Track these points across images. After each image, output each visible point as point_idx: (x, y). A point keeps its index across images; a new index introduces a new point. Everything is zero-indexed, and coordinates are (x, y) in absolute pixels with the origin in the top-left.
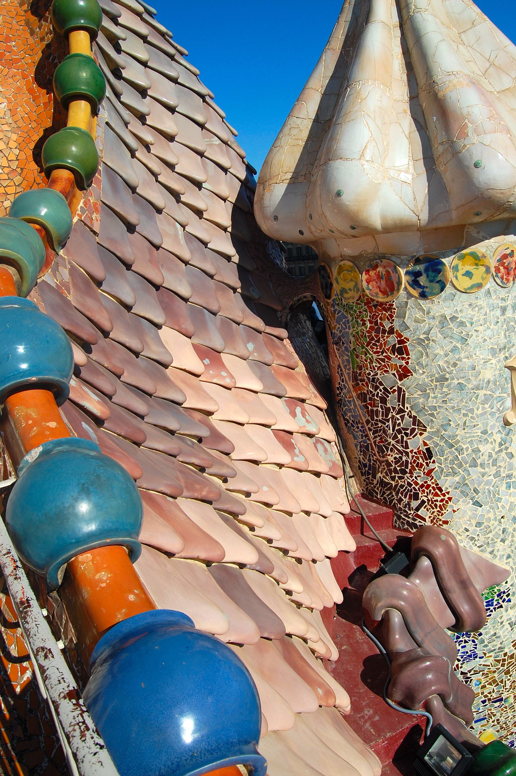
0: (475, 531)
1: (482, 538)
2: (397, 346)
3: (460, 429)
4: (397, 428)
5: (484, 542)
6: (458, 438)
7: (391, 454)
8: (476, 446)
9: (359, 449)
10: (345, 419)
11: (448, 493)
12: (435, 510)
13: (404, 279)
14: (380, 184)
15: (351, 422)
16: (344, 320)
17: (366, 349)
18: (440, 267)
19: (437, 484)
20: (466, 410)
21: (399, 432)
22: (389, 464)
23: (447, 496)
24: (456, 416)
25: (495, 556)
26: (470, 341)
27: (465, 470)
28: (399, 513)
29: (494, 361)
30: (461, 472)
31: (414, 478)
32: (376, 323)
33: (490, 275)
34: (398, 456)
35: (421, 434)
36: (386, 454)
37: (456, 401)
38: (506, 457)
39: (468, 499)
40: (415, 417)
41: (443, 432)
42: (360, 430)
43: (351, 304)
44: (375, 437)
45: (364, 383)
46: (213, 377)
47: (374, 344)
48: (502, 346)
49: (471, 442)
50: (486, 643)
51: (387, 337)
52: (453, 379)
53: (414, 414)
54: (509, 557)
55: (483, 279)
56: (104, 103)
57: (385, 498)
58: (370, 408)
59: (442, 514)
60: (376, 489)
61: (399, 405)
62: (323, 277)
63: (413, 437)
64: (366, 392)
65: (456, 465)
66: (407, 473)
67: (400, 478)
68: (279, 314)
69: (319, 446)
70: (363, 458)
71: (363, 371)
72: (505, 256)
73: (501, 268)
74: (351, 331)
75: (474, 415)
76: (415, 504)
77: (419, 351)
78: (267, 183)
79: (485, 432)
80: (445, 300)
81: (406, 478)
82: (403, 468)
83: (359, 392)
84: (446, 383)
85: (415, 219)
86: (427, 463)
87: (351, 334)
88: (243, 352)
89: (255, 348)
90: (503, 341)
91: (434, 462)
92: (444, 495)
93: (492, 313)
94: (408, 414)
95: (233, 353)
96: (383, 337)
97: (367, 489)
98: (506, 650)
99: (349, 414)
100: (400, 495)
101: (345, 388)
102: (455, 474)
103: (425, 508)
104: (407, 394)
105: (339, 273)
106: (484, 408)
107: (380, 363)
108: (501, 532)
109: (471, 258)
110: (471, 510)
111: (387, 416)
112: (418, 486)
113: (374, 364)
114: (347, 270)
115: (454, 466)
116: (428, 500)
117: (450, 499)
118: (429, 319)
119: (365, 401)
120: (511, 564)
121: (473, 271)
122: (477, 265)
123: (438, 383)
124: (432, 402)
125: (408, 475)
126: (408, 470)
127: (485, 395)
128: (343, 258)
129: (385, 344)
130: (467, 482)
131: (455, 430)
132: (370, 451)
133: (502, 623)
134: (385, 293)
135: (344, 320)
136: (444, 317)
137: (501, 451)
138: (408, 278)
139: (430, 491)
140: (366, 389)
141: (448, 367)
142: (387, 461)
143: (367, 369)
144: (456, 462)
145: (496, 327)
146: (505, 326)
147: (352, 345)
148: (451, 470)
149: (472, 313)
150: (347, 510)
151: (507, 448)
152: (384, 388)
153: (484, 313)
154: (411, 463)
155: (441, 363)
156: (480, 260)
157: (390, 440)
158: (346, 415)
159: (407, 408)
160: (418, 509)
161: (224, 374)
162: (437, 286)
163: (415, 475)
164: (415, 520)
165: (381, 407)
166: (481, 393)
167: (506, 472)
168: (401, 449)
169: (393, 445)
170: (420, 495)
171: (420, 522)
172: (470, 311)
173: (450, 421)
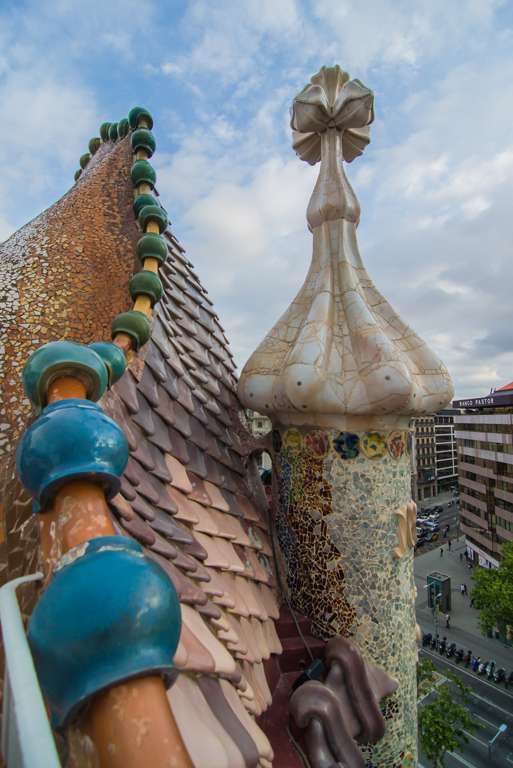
0: (373, 644)
1: (378, 651)
2: (324, 490)
3: (364, 557)
4: (319, 551)
5: (379, 654)
6: (363, 565)
7: (314, 572)
8: (375, 572)
9: (288, 565)
10: (280, 541)
11: (354, 609)
12: (344, 623)
13: (332, 445)
14: (324, 382)
15: (284, 543)
16: (287, 468)
17: (302, 490)
18: (356, 440)
19: (346, 601)
20: (369, 544)
21: (320, 555)
22: (311, 580)
23: (353, 611)
24: (362, 547)
25: (387, 669)
26: (373, 493)
27: (367, 591)
28: (316, 623)
29: (388, 509)
30: (364, 592)
31: (329, 593)
32: (310, 472)
33: (387, 450)
34: (318, 574)
35: (336, 559)
36: (309, 572)
37: (363, 536)
38: (395, 583)
39: (368, 615)
40: (333, 545)
41: (352, 559)
42: (291, 551)
43: (294, 457)
44: (302, 557)
45: (298, 515)
46: (197, 497)
47: (307, 487)
48: (393, 499)
49: (371, 569)
50: (379, 753)
51: (317, 483)
52: (360, 519)
53: (332, 542)
54: (397, 670)
55: (383, 451)
56: (158, 303)
57: (305, 609)
58: (300, 534)
59: (349, 627)
60: (299, 600)
61: (322, 534)
62: (276, 437)
63: (331, 560)
64: (298, 521)
65: (360, 586)
66: (324, 589)
67: (319, 593)
68: (242, 459)
69: (262, 560)
70: (291, 574)
71: (298, 506)
72: (396, 439)
73: (394, 446)
74: (291, 476)
75: (375, 548)
76: (328, 616)
77: (339, 496)
78: (248, 373)
79: (381, 562)
80: (358, 462)
81: (323, 593)
82: (322, 584)
83: (293, 521)
84: (356, 521)
85: (343, 407)
86: (339, 583)
87: (292, 478)
88: (218, 482)
89: (225, 480)
90: (393, 496)
91: (344, 582)
92: (351, 610)
93: (388, 475)
94: (328, 542)
95: (212, 481)
96: (314, 483)
97: (292, 599)
98: (395, 761)
99: (284, 537)
100: (317, 607)
101: (283, 516)
102: (359, 593)
103: (336, 620)
104: (328, 526)
105: (288, 436)
106: (381, 543)
107: (310, 501)
108: (392, 647)
109: (376, 437)
110: (370, 626)
111: (312, 541)
112: (332, 601)
113: (306, 502)
114: (294, 435)
115: (359, 587)
116: (339, 613)
117: (355, 614)
118: (347, 474)
119: (297, 528)
120: (399, 676)
121: (377, 446)
122: (379, 442)
123: (351, 521)
124: (346, 535)
125: (325, 591)
126: (325, 587)
127: (382, 533)
128: (292, 426)
129: (315, 488)
130: (368, 601)
131: (361, 558)
132: (297, 567)
133: (392, 732)
134: (319, 453)
135: (287, 468)
136: (356, 474)
137: (392, 578)
138: (334, 444)
139: (341, 606)
140: (298, 519)
141: (358, 510)
142: (310, 577)
143: (301, 505)
144: (361, 584)
145: (390, 485)
146: (395, 486)
147: (291, 486)
148: (356, 590)
149: (375, 474)
150: (277, 615)
151: (396, 576)
152: (312, 520)
153: (382, 474)
154: (327, 581)
155: (353, 506)
156: (381, 439)
157: (313, 561)
158: (282, 537)
159: (328, 537)
160: (331, 620)
161: (205, 495)
162: (353, 453)
163: (330, 591)
164: (328, 630)
165: (309, 534)
166: (380, 531)
167: (396, 596)
168: (321, 568)
169: (315, 565)
170: (333, 609)
171: (332, 632)
172: (373, 472)
173: (357, 550)
